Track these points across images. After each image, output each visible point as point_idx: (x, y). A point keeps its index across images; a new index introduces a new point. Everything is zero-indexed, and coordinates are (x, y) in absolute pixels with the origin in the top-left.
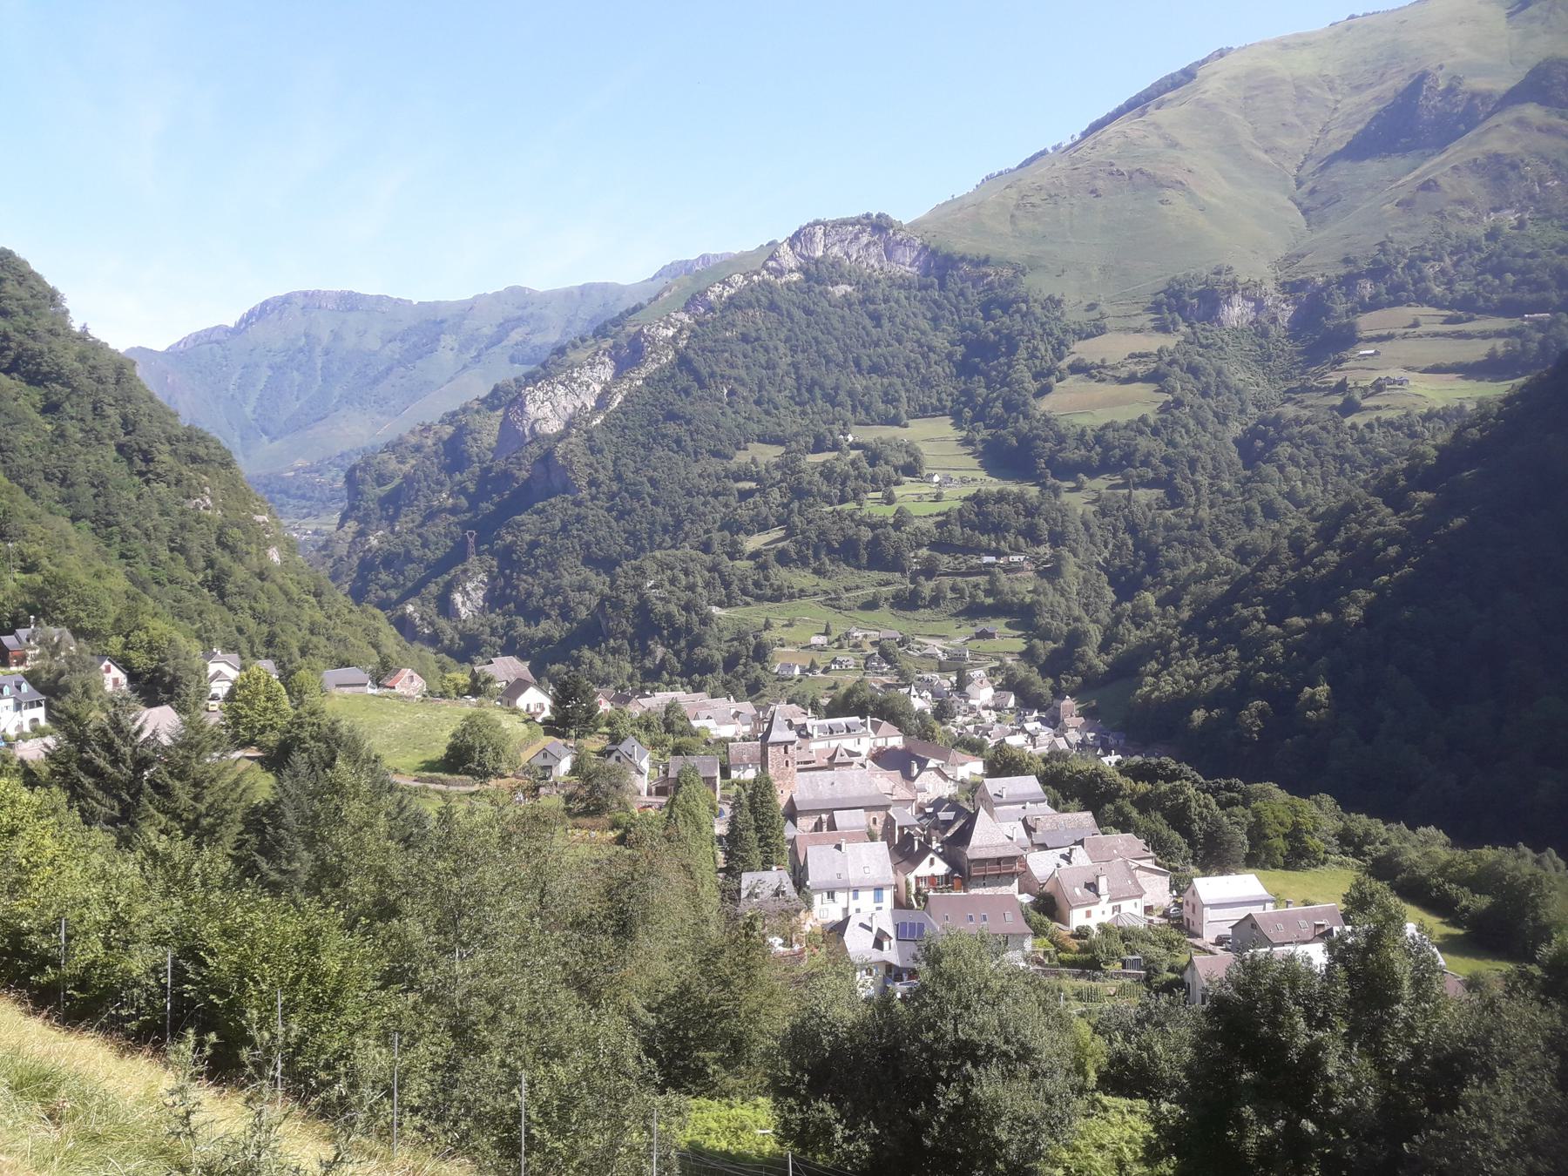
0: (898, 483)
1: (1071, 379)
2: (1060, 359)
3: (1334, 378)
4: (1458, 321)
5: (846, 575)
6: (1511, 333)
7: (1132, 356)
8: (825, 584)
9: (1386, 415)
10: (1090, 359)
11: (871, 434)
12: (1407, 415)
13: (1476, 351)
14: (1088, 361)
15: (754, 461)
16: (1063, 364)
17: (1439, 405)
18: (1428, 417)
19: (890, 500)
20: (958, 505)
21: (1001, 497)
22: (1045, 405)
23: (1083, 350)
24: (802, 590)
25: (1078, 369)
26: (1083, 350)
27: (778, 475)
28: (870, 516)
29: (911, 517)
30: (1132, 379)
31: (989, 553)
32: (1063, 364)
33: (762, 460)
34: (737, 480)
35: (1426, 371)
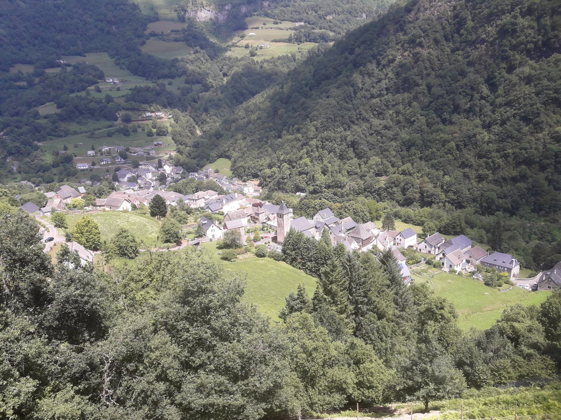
0: (98, 83)
1: (152, 38)
2: (145, 30)
3: (244, 42)
4: (277, 23)
5: (92, 125)
6: (295, 29)
7: (172, 31)
8: (84, 128)
9: (267, 58)
10: (159, 31)
11: (75, 60)
12: (273, 58)
13: (287, 34)
14: (157, 32)
15: (20, 72)
16: (147, 32)
17: (281, 55)
18: (279, 58)
19: (99, 90)
20: (130, 92)
21: (147, 89)
22: (144, 49)
23: (152, 27)
24: (75, 132)
25: (153, 35)
26: (152, 27)
27: (37, 80)
28: (94, 98)
29: (112, 98)
30: (176, 40)
31: (148, 111)
32: (147, 32)
33: (24, 72)
34: (15, 81)
35: (272, 41)
